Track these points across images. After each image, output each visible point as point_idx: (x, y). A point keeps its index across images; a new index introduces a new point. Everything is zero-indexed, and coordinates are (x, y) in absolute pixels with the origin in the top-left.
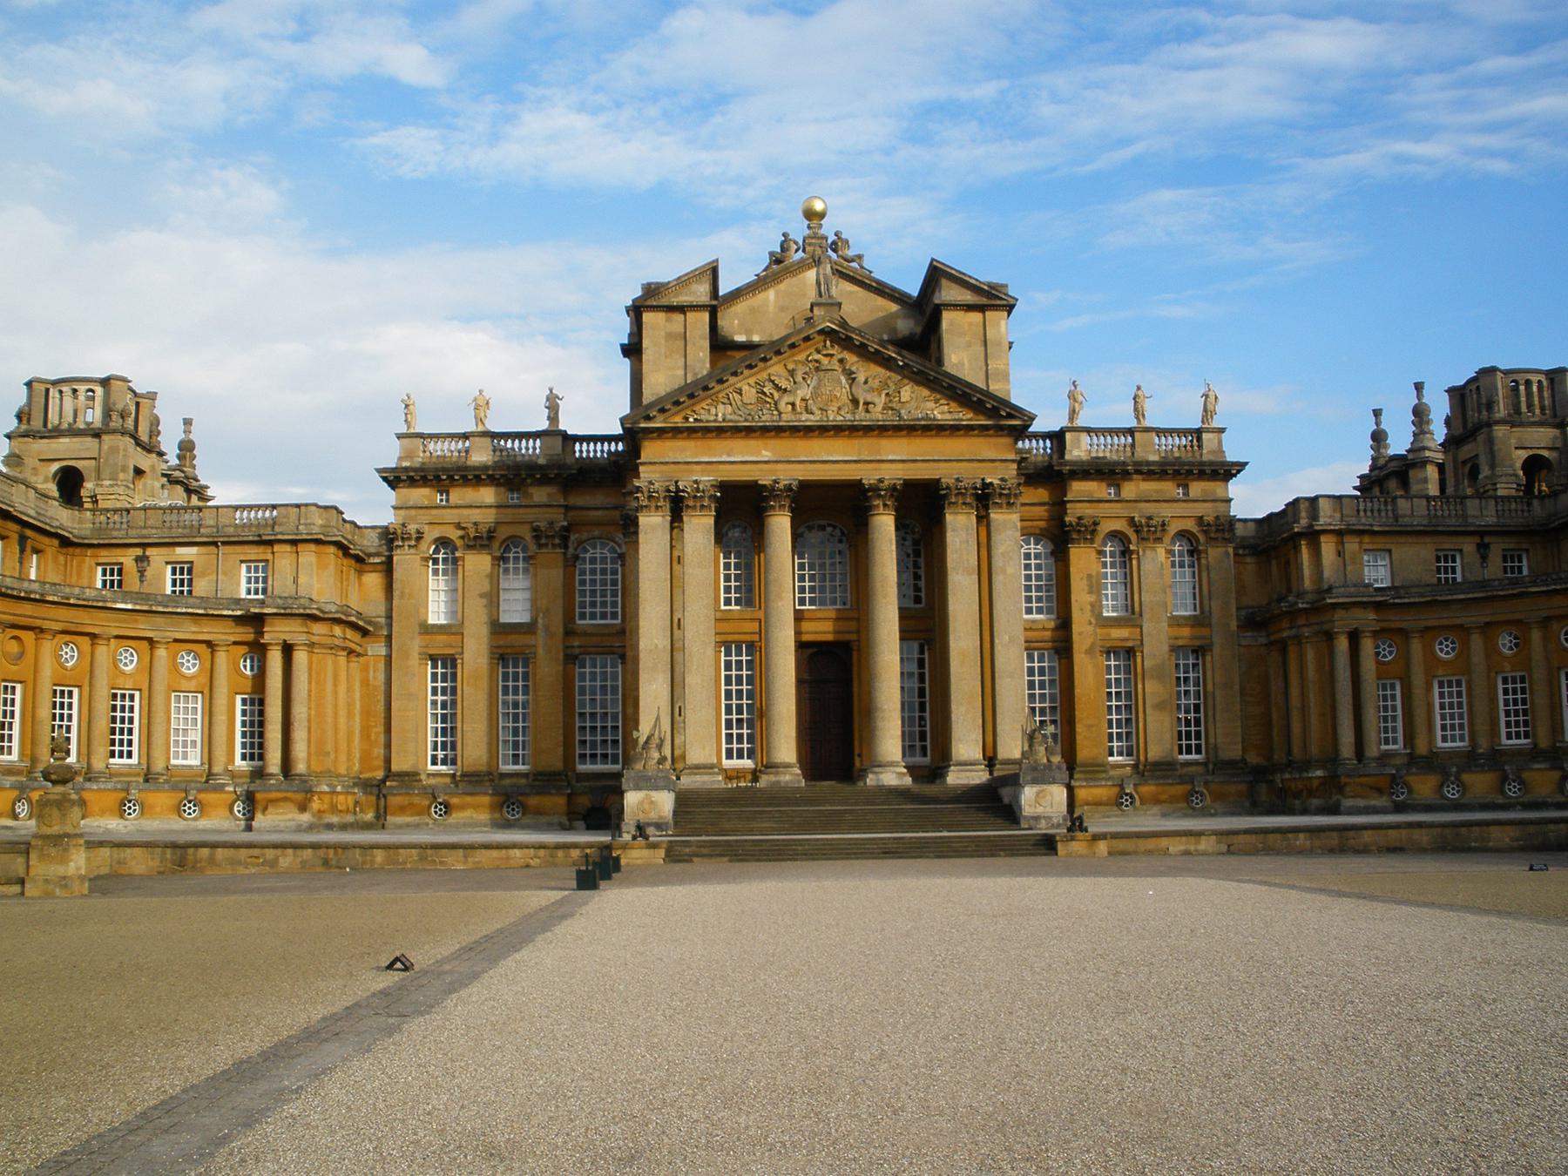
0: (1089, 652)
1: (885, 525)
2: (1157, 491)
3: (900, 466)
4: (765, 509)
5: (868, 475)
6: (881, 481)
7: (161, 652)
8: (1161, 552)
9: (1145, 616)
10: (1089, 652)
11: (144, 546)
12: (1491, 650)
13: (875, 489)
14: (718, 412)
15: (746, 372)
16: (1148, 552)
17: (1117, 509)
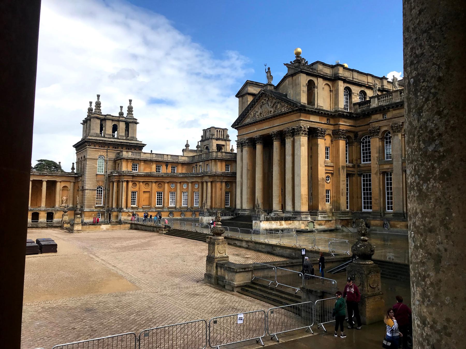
0: (376, 174)
1: (276, 144)
2: (399, 113)
3: (277, 127)
4: (256, 144)
5: (270, 131)
6: (273, 132)
7: (190, 184)
8: (400, 135)
9: (394, 160)
10: (376, 174)
11: (196, 163)
12: (193, 187)
13: (272, 135)
14: (248, 121)
15: (252, 109)
16: (395, 137)
17: (385, 123)
